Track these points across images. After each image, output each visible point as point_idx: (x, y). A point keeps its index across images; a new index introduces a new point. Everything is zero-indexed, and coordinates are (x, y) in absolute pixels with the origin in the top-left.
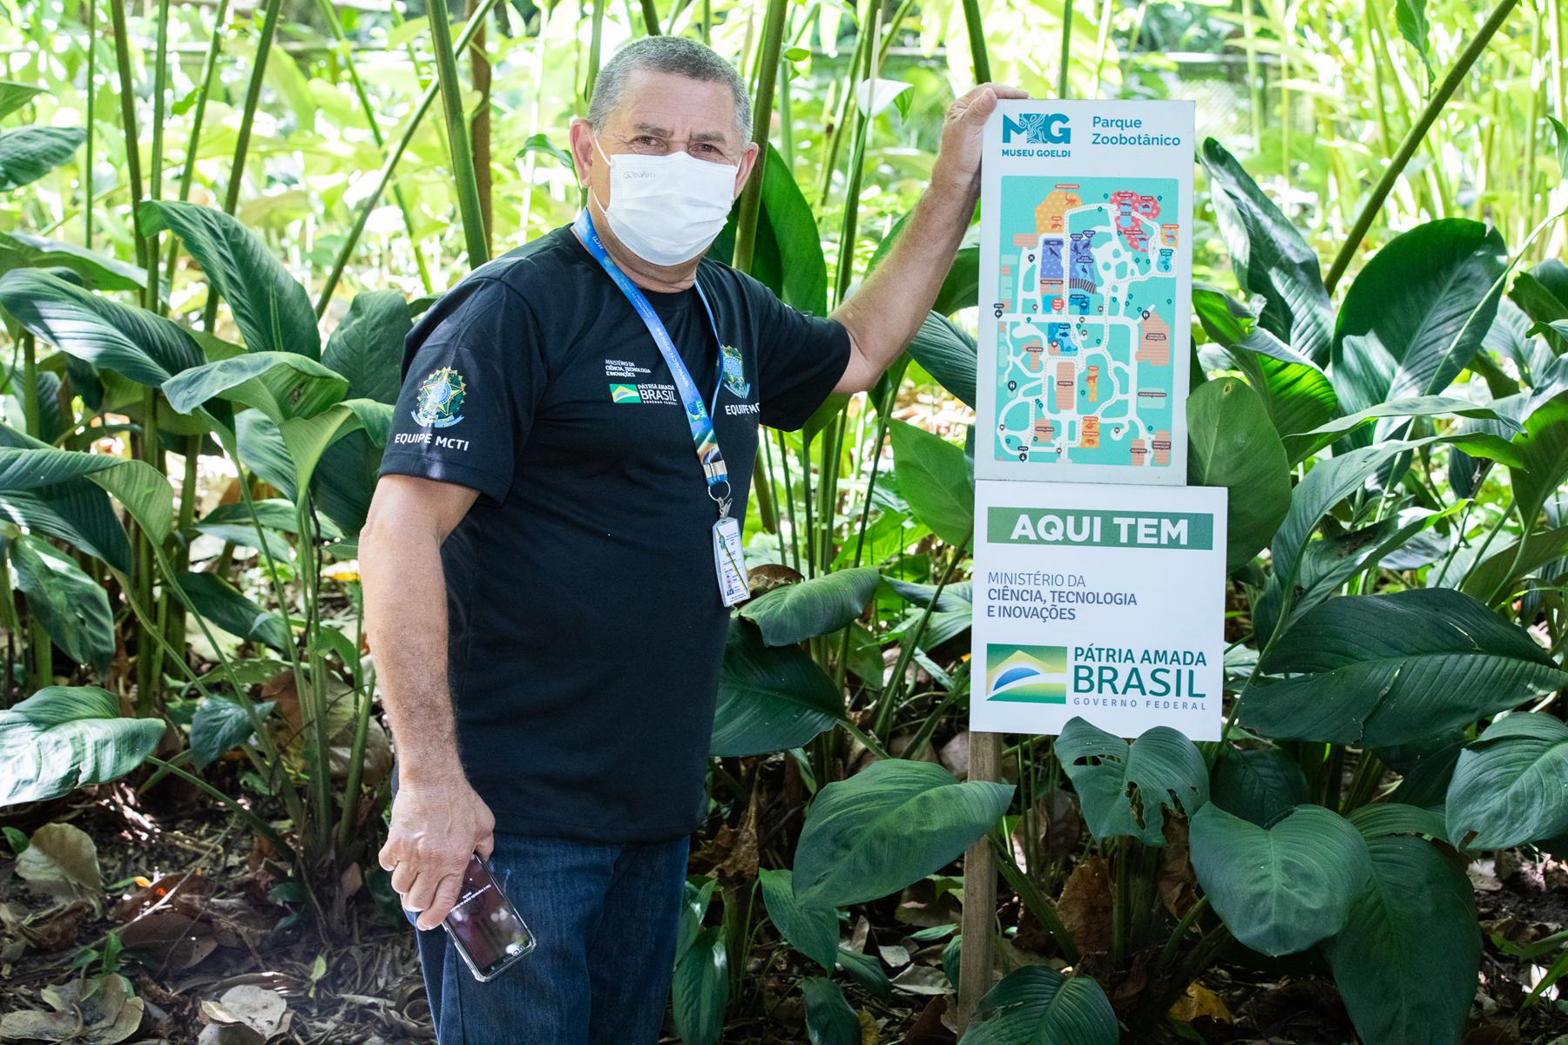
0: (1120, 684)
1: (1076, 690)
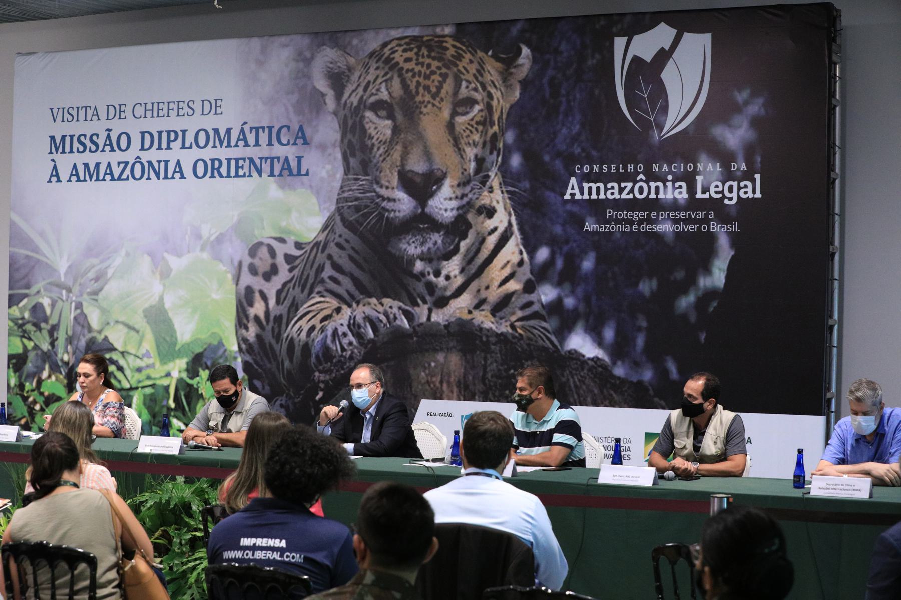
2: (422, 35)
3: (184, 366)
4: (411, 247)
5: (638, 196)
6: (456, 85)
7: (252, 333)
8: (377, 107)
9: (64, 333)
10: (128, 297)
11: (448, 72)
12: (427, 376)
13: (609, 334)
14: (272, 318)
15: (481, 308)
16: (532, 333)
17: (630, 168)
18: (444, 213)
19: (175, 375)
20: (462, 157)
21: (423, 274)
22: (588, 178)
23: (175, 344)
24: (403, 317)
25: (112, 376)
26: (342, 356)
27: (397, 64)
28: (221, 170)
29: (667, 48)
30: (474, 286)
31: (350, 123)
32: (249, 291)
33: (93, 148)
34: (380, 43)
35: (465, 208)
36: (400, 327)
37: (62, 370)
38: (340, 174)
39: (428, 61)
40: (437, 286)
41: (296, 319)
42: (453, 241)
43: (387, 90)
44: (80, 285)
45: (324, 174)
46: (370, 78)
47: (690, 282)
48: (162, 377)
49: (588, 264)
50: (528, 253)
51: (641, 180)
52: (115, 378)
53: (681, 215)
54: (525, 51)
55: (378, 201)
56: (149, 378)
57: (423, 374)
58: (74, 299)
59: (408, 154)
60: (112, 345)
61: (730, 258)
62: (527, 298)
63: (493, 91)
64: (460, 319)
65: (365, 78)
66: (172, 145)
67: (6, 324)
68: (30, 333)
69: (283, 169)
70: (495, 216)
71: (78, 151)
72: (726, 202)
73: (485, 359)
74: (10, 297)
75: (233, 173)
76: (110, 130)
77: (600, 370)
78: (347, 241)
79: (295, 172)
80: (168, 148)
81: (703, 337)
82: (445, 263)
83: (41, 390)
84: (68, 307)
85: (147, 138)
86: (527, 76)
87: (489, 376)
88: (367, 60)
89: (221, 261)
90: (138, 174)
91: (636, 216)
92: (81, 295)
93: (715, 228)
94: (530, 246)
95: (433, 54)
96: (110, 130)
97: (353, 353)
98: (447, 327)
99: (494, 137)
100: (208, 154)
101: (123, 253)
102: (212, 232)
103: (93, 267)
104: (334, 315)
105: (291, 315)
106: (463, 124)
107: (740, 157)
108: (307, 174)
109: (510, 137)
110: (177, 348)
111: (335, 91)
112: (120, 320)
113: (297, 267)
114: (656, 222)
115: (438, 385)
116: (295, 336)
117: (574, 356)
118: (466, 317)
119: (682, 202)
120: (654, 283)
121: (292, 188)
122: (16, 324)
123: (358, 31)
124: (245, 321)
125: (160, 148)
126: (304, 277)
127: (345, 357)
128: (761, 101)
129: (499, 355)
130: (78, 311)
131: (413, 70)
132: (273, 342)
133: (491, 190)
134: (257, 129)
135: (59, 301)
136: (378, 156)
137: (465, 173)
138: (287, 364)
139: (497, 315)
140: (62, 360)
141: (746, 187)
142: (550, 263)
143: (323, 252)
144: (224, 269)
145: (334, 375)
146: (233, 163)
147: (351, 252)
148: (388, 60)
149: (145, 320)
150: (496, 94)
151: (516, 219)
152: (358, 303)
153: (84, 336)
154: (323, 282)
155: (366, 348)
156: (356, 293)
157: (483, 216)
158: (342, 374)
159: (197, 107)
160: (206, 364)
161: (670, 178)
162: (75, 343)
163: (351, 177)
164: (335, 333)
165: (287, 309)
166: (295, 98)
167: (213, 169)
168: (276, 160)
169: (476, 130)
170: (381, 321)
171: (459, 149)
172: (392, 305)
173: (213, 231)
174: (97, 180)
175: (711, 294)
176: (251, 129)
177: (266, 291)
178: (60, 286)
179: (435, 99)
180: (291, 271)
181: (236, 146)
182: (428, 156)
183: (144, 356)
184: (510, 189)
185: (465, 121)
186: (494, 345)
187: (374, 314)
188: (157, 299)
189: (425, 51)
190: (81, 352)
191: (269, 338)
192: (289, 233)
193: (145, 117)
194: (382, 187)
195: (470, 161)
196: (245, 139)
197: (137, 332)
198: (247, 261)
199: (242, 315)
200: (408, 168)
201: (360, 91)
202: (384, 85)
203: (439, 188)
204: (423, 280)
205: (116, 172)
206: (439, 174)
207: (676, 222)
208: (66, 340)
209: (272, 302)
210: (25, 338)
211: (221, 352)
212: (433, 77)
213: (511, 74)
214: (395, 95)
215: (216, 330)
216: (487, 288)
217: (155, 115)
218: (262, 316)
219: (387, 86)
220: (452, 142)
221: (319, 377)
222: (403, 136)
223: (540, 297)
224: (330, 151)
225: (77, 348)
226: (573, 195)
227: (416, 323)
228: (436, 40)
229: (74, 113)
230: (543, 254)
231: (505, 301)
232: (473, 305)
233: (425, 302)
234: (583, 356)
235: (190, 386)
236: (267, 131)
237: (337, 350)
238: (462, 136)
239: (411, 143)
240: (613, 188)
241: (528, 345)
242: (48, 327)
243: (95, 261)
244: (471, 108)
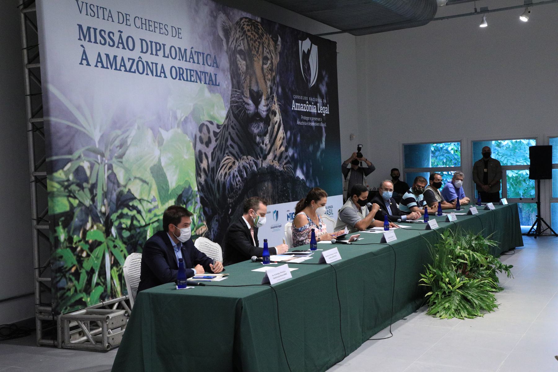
7: (202, 179)
8: (241, 52)
9: (101, 190)
10: (141, 159)
12: (263, 194)
13: (305, 169)
14: (210, 169)
18: (263, 112)
22: (297, 101)
23: (168, 190)
25: (134, 219)
28: (183, 75)
34: (240, 18)
35: (269, 110)
37: (101, 219)
38: (230, 88)
39: (254, 33)
41: (219, 169)
44: (110, 150)
56: (155, 215)
58: (106, 161)
60: (133, 195)
63: (273, 55)
68: (75, 192)
73: (278, 183)
78: (235, 125)
80: (157, 55)
82: (265, 137)
84: (103, 168)
89: (187, 134)
91: (307, 118)
92: (111, 159)
94: (286, 131)
100: (178, 63)
101: (136, 127)
103: (118, 136)
104: (233, 165)
105: (218, 167)
108: (219, 85)
110: (169, 193)
111: (226, 39)
112: (137, 176)
113: (218, 138)
118: (272, 164)
122: (63, 186)
124: (200, 172)
125: (152, 54)
126: (221, 145)
130: (110, 171)
132: (212, 183)
134: (198, 53)
135: (96, 164)
138: (217, 195)
140: (101, 212)
143: (227, 130)
144: (189, 139)
146: (189, 71)
147: (236, 131)
148: (243, 28)
149: (151, 175)
150: (274, 57)
155: (244, 182)
156: (239, 153)
160: (184, 201)
162: (109, 196)
164: (234, 174)
165: (216, 164)
167: (180, 74)
170: (248, 168)
171: (265, 81)
173: (182, 115)
175: (323, 151)
176: (195, 52)
177: (207, 153)
178: (96, 152)
180: (216, 141)
183: (152, 200)
188: (157, 160)
189: (253, 28)
190: (114, 203)
191: (210, 182)
192: (214, 118)
194: (244, 97)
197: (148, 184)
198: (199, 135)
199: (198, 168)
201: (235, 41)
202: (242, 41)
205: (128, 65)
207: (315, 122)
208: (103, 194)
209: (210, 159)
211: (190, 193)
215: (187, 179)
216: (276, 150)
221: (229, 201)
225: (111, 201)
227: (258, 168)
228: (256, 23)
241: (288, 175)
242: (89, 186)
243: (119, 132)
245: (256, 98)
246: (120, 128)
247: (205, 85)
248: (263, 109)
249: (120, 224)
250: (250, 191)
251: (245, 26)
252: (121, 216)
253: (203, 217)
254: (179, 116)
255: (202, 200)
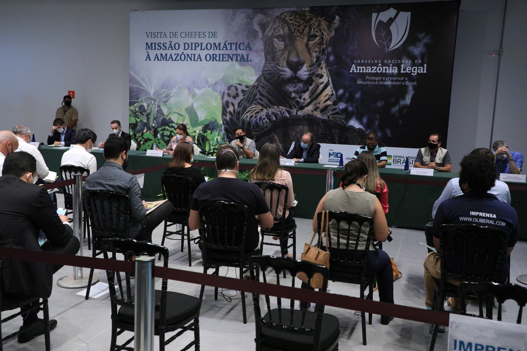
0: (402, 162)
1: (393, 163)
2: (297, 10)
3: (201, 129)
4: (291, 88)
5: (378, 71)
6: (309, 30)
7: (228, 117)
8: (279, 37)
9: (153, 116)
10: (179, 103)
11: (306, 24)
12: (295, 134)
13: (365, 120)
14: (236, 112)
15: (317, 110)
16: (336, 119)
17: (376, 61)
19: (198, 132)
20: (311, 56)
21: (295, 98)
23: (198, 121)
24: (287, 113)
26: (263, 126)
27: (287, 21)
29: (393, 17)
30: (314, 102)
31: (268, 42)
32: (227, 102)
33: (164, 48)
34: (281, 13)
36: (285, 116)
37: (152, 129)
38: (263, 61)
39: (299, 20)
40: (300, 102)
41: (245, 113)
42: (306, 87)
43: (283, 31)
44: (159, 98)
45: (257, 61)
46: (276, 26)
47: (397, 102)
48: (192, 133)
49: (358, 96)
50: (335, 91)
51: (380, 66)
52: (174, 132)
53: (395, 79)
54: (337, 18)
55: (278, 71)
57: (294, 133)
58: (157, 104)
59: (290, 54)
61: (413, 94)
62: (334, 107)
63: (324, 32)
64: (308, 114)
65: (274, 26)
66: (197, 48)
67: (128, 112)
69: (241, 59)
70: (323, 77)
71: (158, 49)
72: (412, 74)
73: (318, 128)
74: (130, 102)
75: (221, 59)
76: (172, 42)
77: (361, 132)
78: (266, 86)
79: (246, 60)
80: (195, 49)
81: (401, 122)
82: (303, 94)
83: (143, 137)
85: (187, 45)
86: (337, 27)
87: (319, 134)
88: (275, 19)
90: (183, 58)
91: (377, 79)
92: (160, 102)
93: (407, 83)
94: (336, 88)
95: (301, 18)
96: (172, 42)
97: (267, 125)
98: (303, 116)
99: (324, 49)
100: (211, 52)
101: (177, 87)
102: (213, 81)
103: (165, 92)
104: (260, 111)
105: (243, 111)
106: (312, 44)
107: (419, 58)
108: (251, 61)
109: (330, 49)
112: (176, 112)
114: (385, 81)
115: (299, 137)
116: (245, 119)
117: (351, 128)
119: (395, 74)
120: (383, 103)
121: (244, 66)
123: (272, 8)
124: (225, 113)
126: (249, 98)
127: (264, 126)
128: (428, 37)
129: (323, 127)
130: (159, 108)
131: (293, 23)
132: (236, 121)
133: (322, 68)
134: (231, 44)
136: (278, 55)
137: (312, 62)
139: (323, 113)
140: (152, 126)
141: (420, 69)
142: (343, 95)
143: (256, 89)
144: (218, 94)
145: (260, 133)
146: (221, 56)
148: (283, 20)
149: (186, 112)
151: (331, 79)
152: (270, 108)
153: (161, 117)
154: (256, 100)
156: (269, 104)
157: (318, 78)
158: (263, 133)
159: (207, 34)
161: (391, 65)
163: (267, 62)
164: (261, 117)
165: (242, 109)
166: (246, 32)
167: (213, 58)
168: (238, 56)
169: (317, 46)
170: (278, 114)
171: (310, 53)
172: (283, 109)
174: (166, 60)
175: (405, 107)
176: (229, 43)
177: (234, 103)
178: (151, 99)
179: (301, 35)
180: (244, 95)
181: (223, 49)
182: (298, 55)
184: (329, 68)
185: (313, 43)
186: (321, 123)
187: (275, 112)
188: (191, 104)
189: (298, 17)
190: (160, 123)
191: (234, 119)
192: (243, 82)
193: (186, 37)
194: (280, 66)
195: (314, 58)
196: (226, 47)
197: (183, 116)
198: (227, 91)
199: (224, 111)
200: (290, 60)
201: (272, 31)
202: (281, 29)
203: (302, 67)
204: (295, 100)
205: (174, 58)
206: (302, 62)
207: (392, 81)
208: (154, 118)
209: (236, 107)
210: (137, 117)
212: (301, 27)
213: (331, 26)
214: (286, 33)
215: (214, 116)
216: (319, 103)
217: (190, 36)
218: (232, 111)
219: (282, 29)
220: (307, 50)
222: (288, 48)
223: (339, 106)
224: (260, 52)
226: (353, 71)
227: (292, 115)
229: (156, 34)
230: (341, 92)
231: (326, 107)
232: (314, 109)
233: (295, 108)
234: (355, 128)
235: (204, 136)
236: (235, 44)
237: (261, 124)
238: (311, 48)
239: (292, 50)
240: (369, 68)
241: (334, 123)
242: (146, 114)
243: (166, 90)
244: (315, 38)
245: (295, 67)
246: (166, 88)
247: (237, 62)
248: (304, 73)
249: (163, 133)
250: (279, 130)
251: (287, 18)
252: (164, 130)
253: (226, 140)
254: (210, 81)
255: (226, 130)
